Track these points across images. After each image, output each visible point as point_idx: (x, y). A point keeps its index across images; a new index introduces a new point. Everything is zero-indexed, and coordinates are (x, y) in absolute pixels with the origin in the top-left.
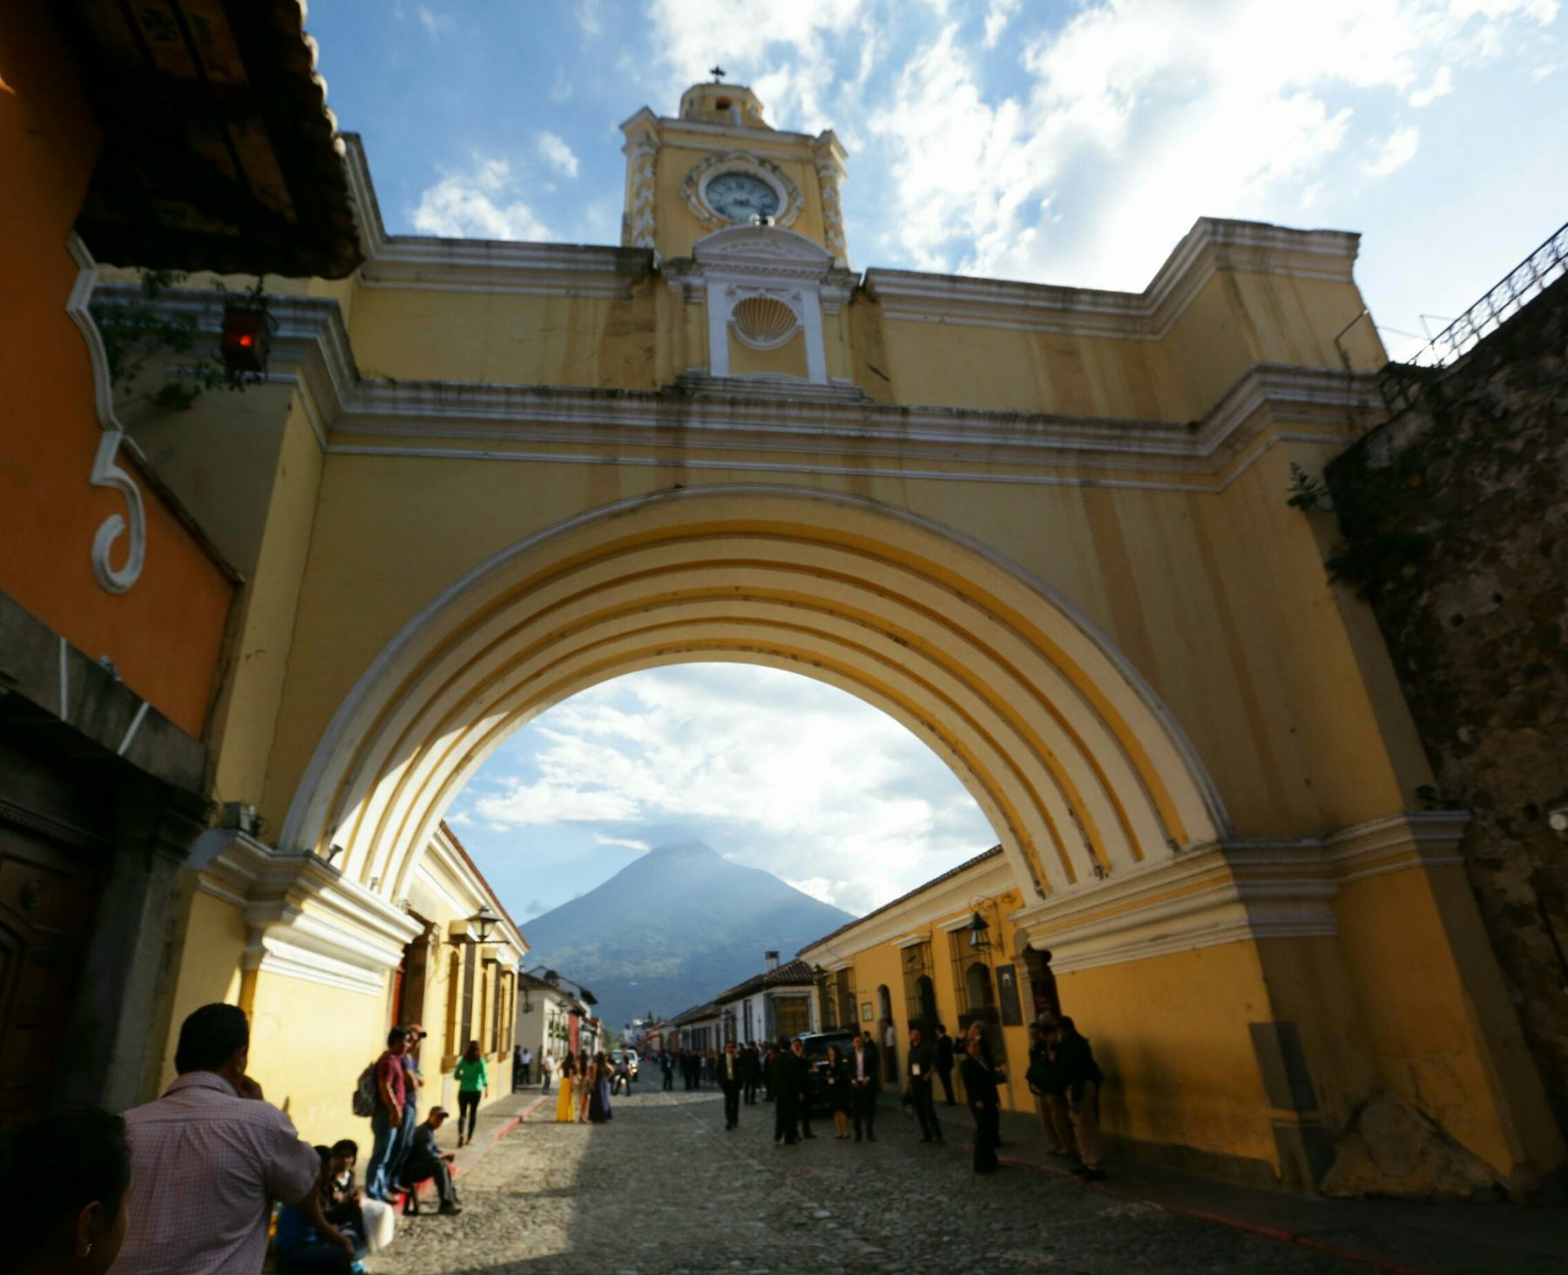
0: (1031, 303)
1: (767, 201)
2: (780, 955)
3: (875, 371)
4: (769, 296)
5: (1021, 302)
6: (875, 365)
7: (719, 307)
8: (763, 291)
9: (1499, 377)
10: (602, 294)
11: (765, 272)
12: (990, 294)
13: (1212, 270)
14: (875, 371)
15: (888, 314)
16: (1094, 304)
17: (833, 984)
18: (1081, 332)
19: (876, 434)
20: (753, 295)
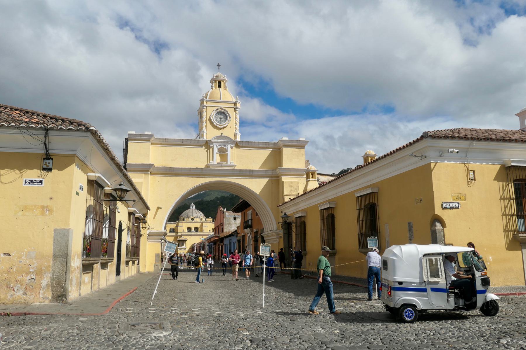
4: (223, 147)
7: (216, 149)
8: (222, 146)
20: (221, 147)
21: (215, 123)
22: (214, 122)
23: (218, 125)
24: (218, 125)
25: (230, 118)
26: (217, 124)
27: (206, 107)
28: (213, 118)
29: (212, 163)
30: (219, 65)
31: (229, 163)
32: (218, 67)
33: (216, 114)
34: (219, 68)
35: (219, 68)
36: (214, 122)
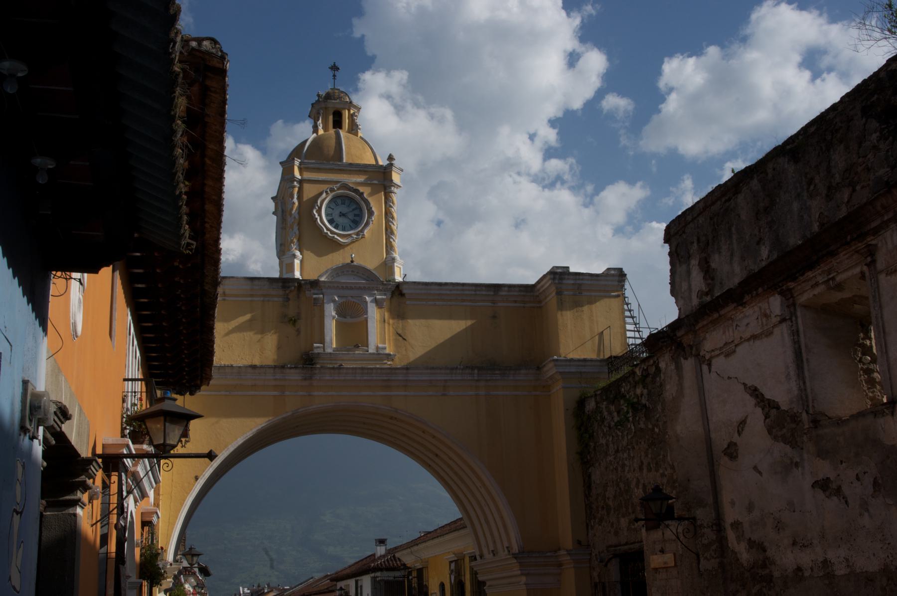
0: (478, 293)
1: (357, 212)
2: (388, 542)
3: (400, 335)
5: (473, 293)
6: (400, 332)
9: (605, 403)
10: (276, 299)
11: (352, 288)
12: (457, 290)
13: (554, 294)
14: (400, 335)
15: (408, 302)
16: (509, 291)
17: (414, 577)
18: (500, 304)
19: (393, 378)
21: (328, 229)
22: (323, 226)
23: (336, 236)
24: (336, 236)
25: (371, 213)
26: (332, 232)
27: (301, 182)
28: (320, 215)
29: (321, 351)
30: (335, 68)
31: (372, 350)
32: (331, 73)
33: (330, 201)
34: (334, 76)
35: (334, 76)
36: (323, 226)
